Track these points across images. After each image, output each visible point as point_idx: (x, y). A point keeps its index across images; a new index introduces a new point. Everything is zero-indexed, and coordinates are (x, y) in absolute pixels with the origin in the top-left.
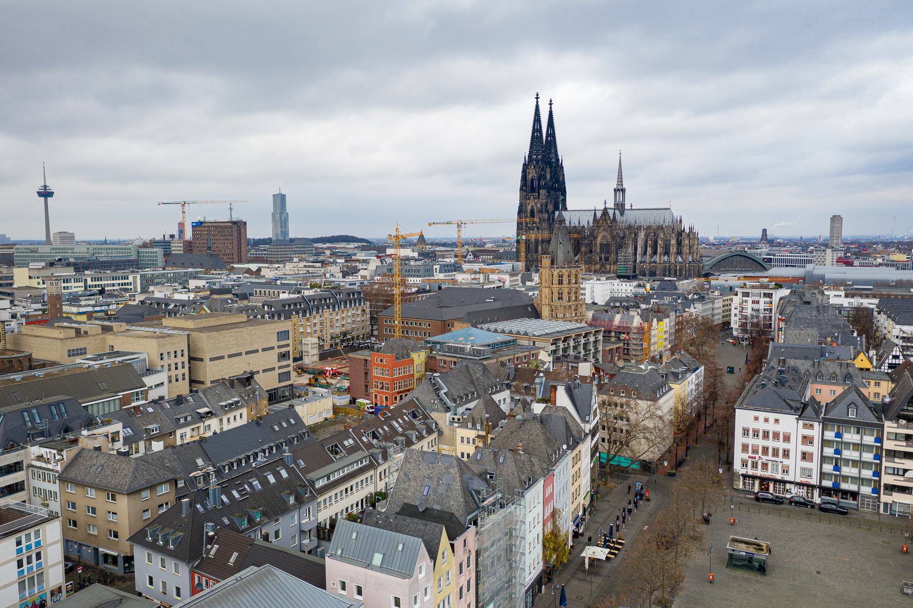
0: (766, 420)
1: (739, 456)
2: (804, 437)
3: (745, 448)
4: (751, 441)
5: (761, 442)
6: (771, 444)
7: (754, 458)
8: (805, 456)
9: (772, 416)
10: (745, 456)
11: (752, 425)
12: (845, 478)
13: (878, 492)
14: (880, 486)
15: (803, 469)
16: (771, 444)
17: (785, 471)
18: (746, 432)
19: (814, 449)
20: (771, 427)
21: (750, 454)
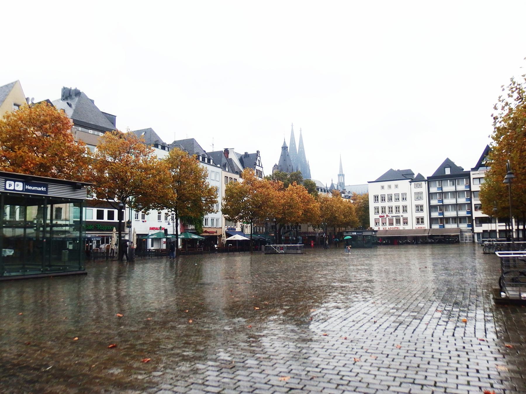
0: (390, 187)
1: (373, 217)
2: (415, 193)
3: (377, 209)
4: (380, 204)
5: (387, 204)
6: (394, 204)
7: (384, 216)
10: (377, 216)
11: (380, 193)
12: (447, 220)
13: (472, 226)
14: (473, 220)
16: (394, 204)
17: (406, 223)
18: (376, 198)
19: (424, 202)
21: (380, 214)
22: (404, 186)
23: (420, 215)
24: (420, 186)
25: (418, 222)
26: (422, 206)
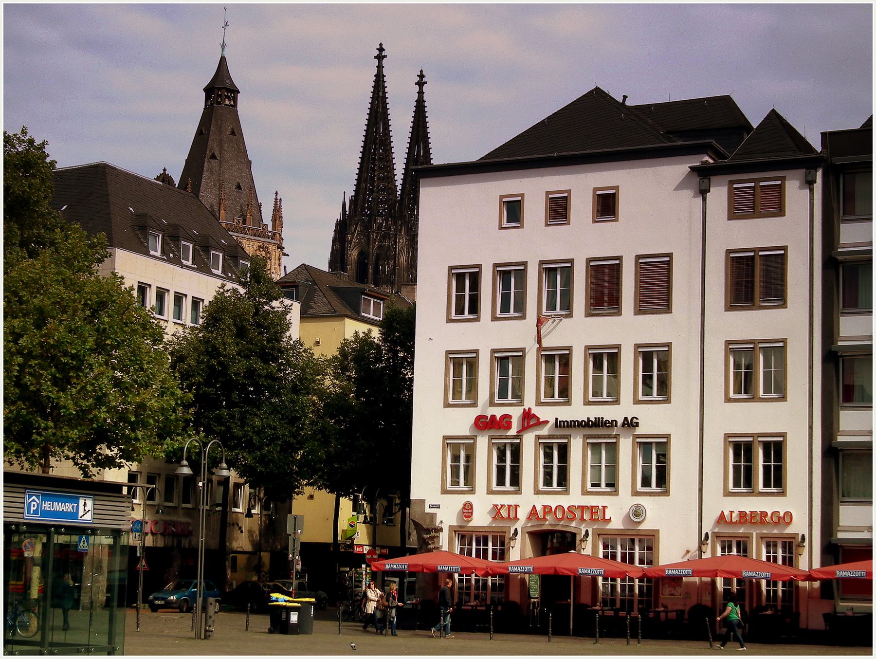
1: (434, 421)
4: (487, 335)
7: (505, 422)
8: (753, 371)
9: (581, 185)
10: (461, 422)
15: (742, 449)
16: (579, 332)
20: (583, 241)
21: (483, 408)
22: (659, 208)
23: (757, 418)
24: (775, 206)
25: (744, 478)
26: (776, 351)
